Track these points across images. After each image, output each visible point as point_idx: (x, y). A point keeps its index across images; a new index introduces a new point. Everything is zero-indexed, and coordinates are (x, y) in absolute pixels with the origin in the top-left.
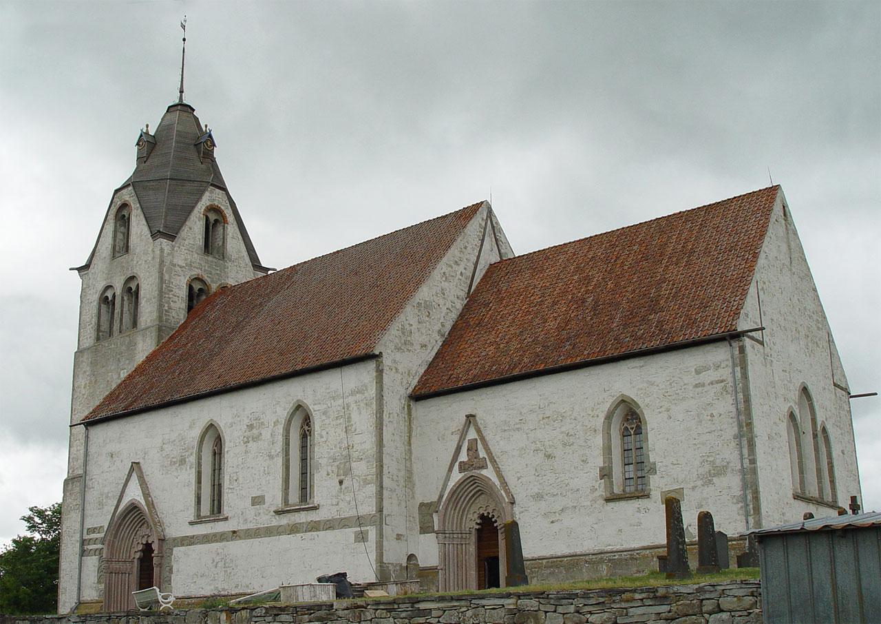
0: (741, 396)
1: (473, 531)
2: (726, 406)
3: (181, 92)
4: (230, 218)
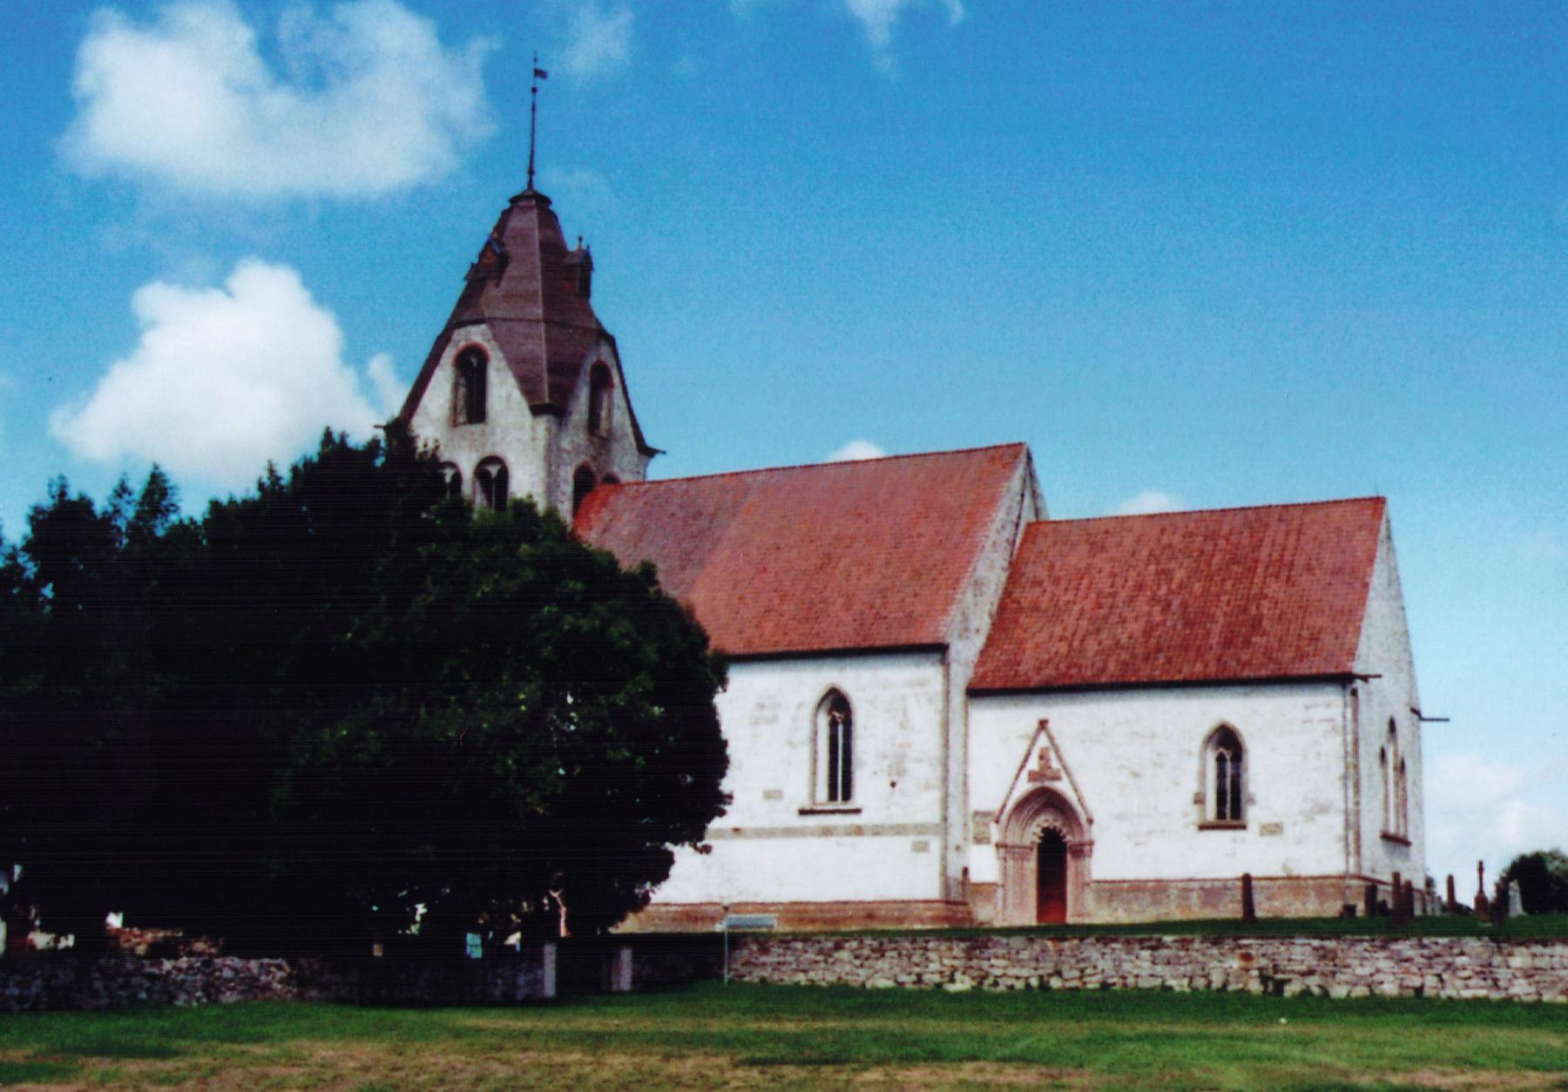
0: (1350, 738)
2: (1334, 746)
3: (531, 172)
4: (616, 380)
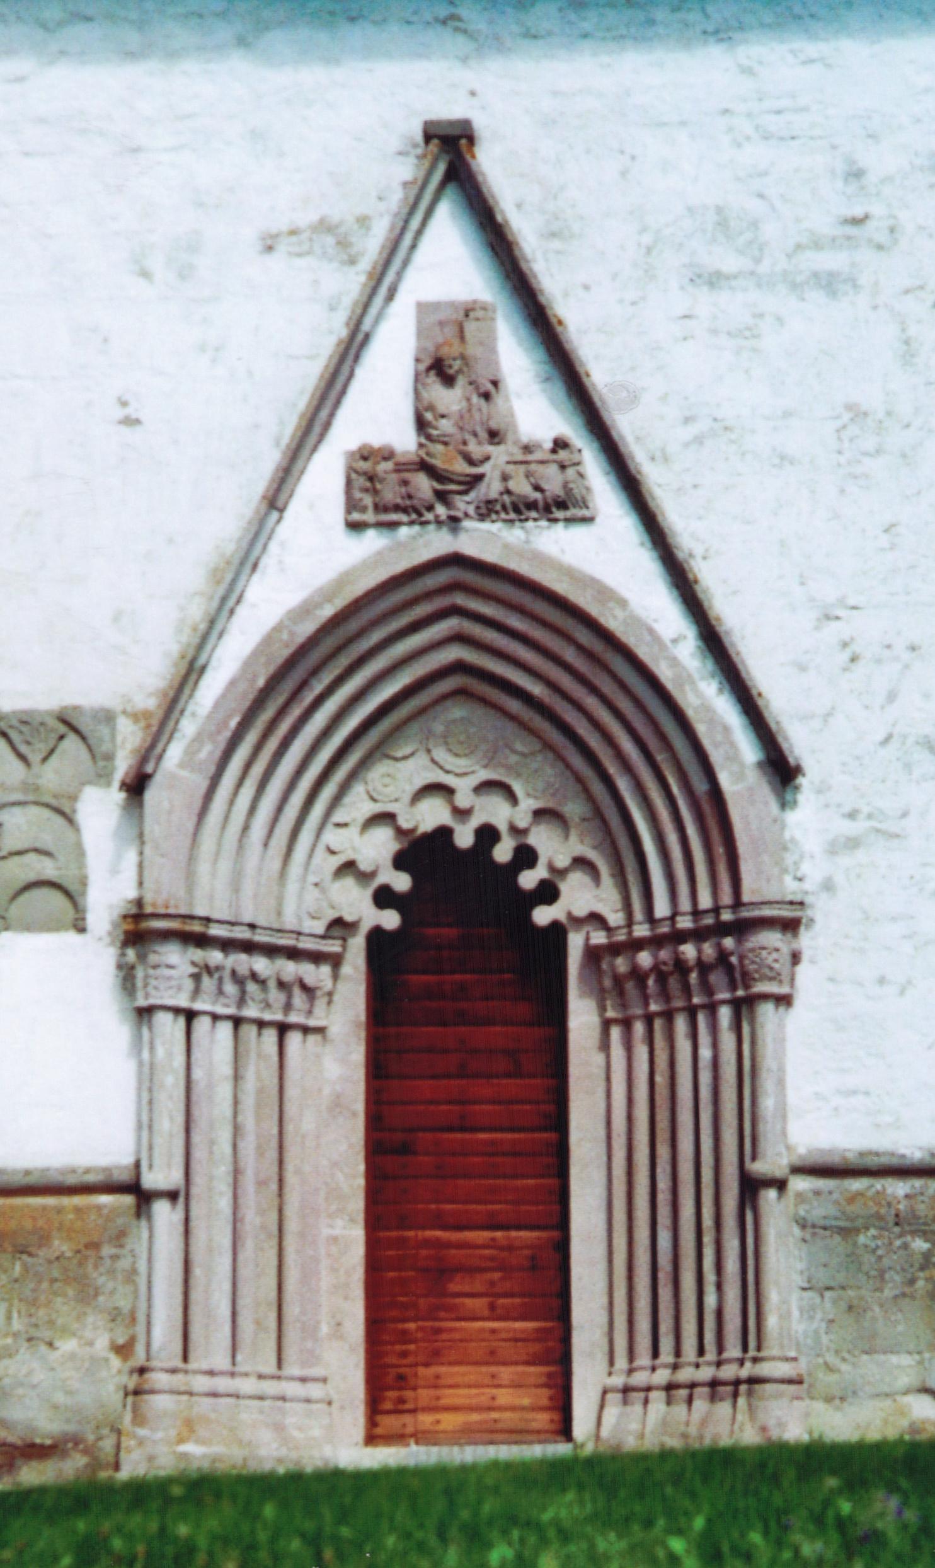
1: (356, 950)
